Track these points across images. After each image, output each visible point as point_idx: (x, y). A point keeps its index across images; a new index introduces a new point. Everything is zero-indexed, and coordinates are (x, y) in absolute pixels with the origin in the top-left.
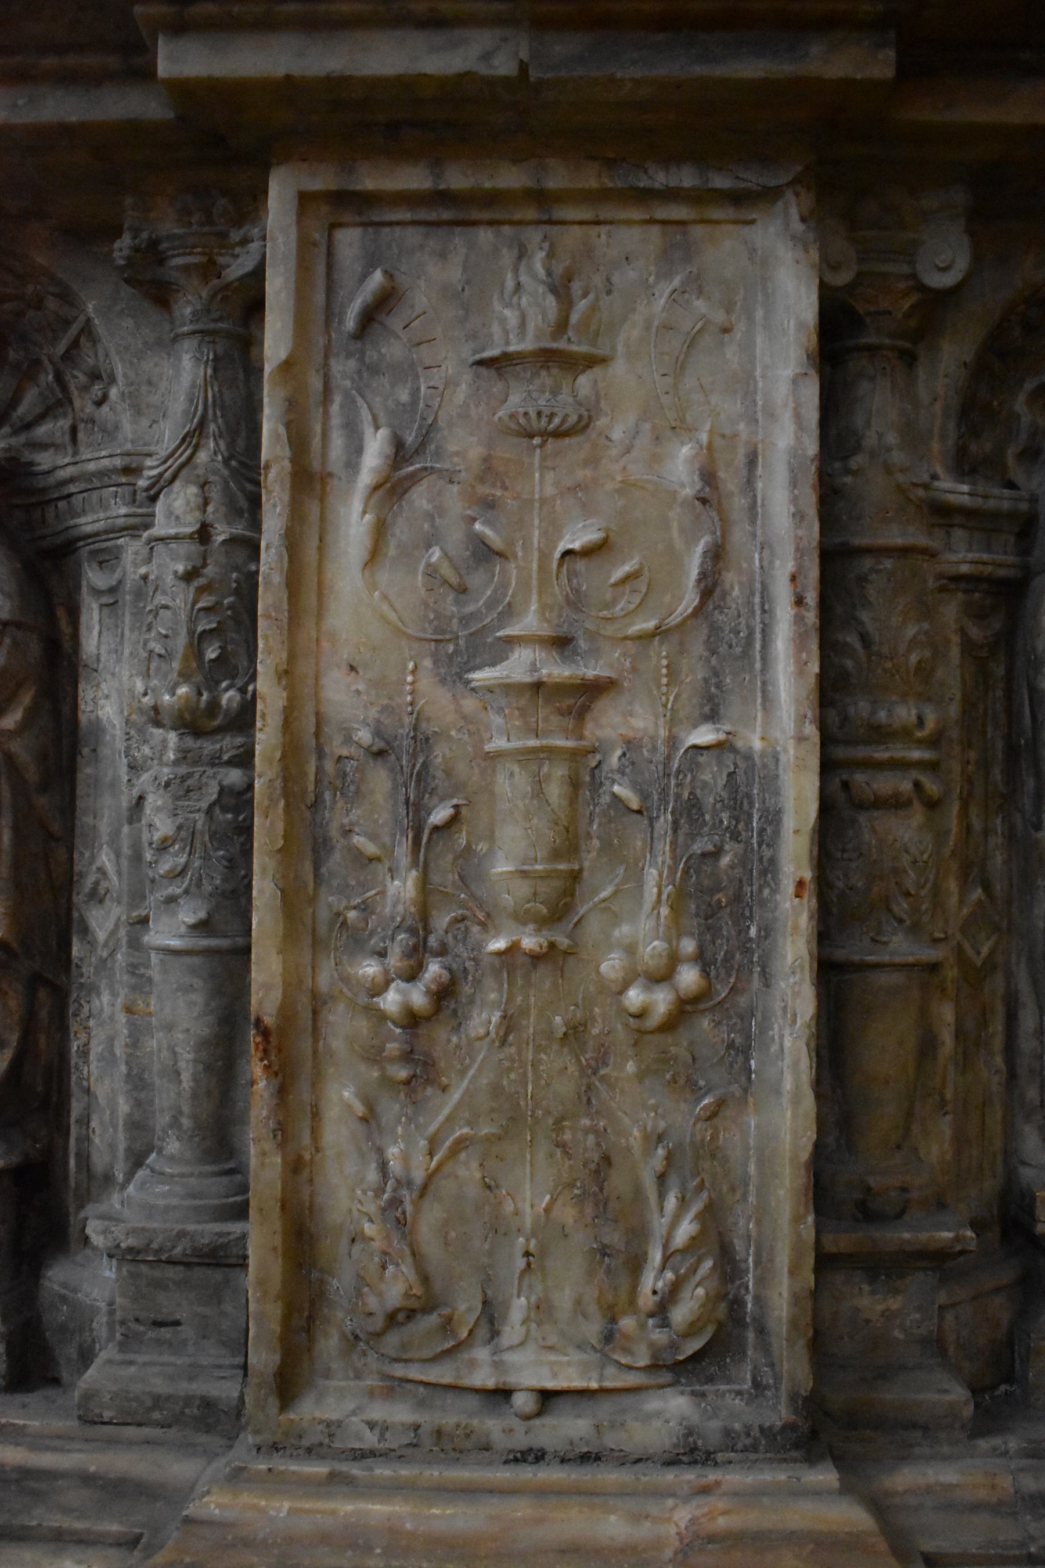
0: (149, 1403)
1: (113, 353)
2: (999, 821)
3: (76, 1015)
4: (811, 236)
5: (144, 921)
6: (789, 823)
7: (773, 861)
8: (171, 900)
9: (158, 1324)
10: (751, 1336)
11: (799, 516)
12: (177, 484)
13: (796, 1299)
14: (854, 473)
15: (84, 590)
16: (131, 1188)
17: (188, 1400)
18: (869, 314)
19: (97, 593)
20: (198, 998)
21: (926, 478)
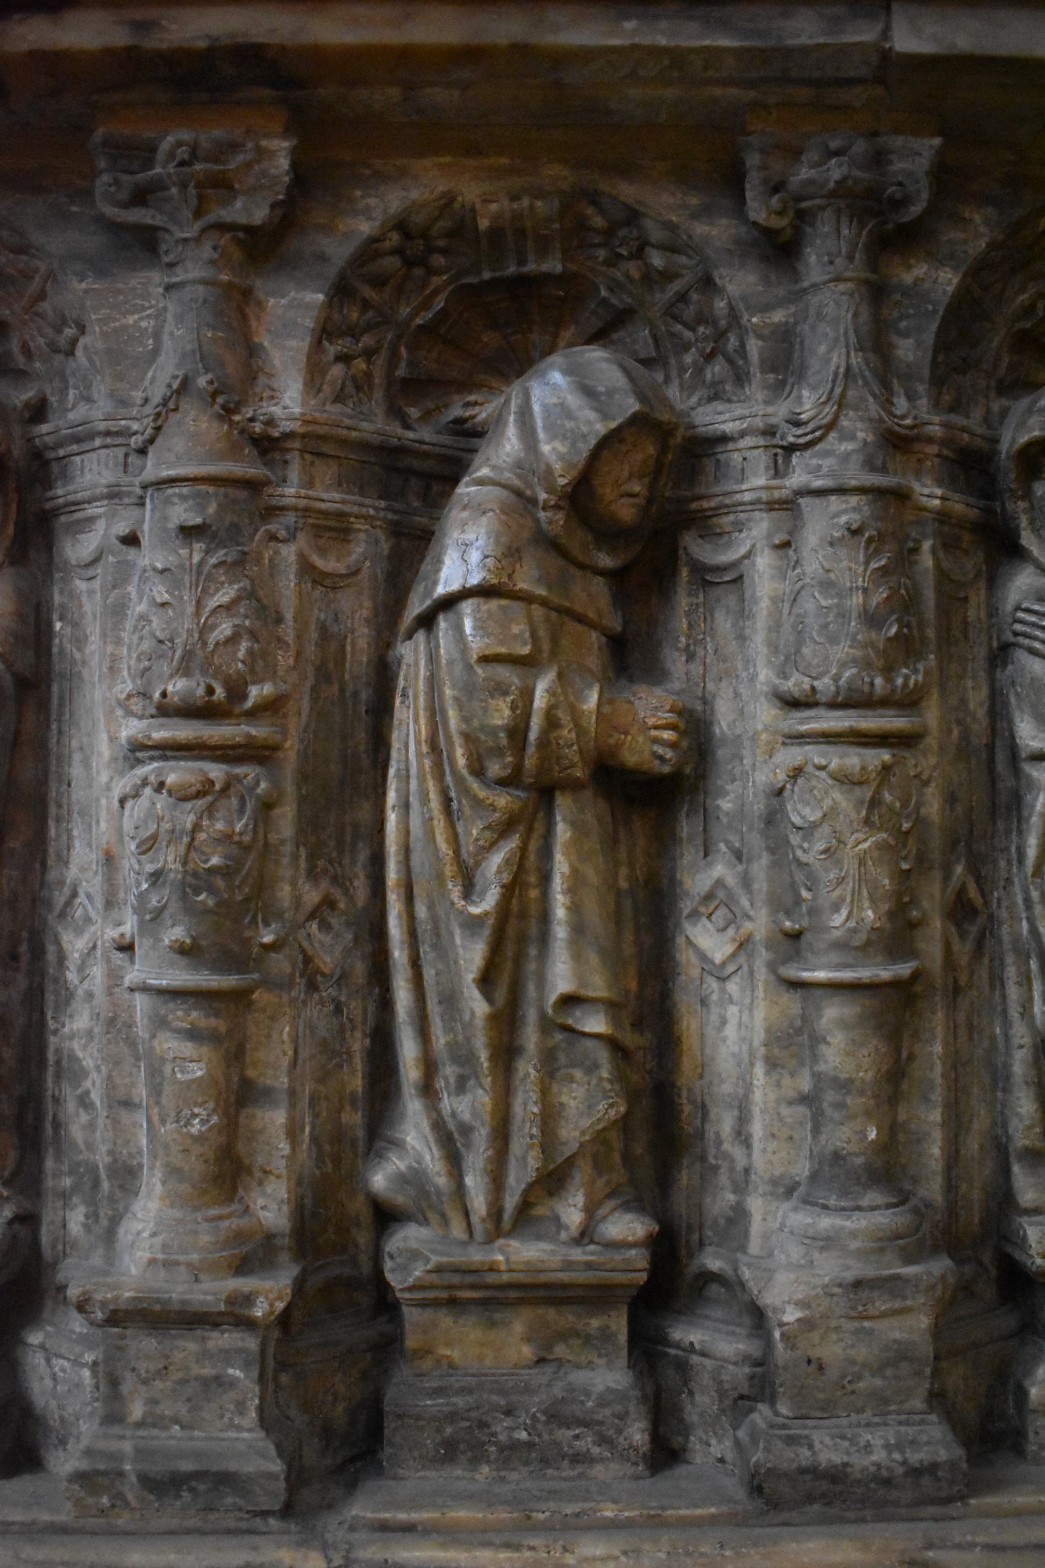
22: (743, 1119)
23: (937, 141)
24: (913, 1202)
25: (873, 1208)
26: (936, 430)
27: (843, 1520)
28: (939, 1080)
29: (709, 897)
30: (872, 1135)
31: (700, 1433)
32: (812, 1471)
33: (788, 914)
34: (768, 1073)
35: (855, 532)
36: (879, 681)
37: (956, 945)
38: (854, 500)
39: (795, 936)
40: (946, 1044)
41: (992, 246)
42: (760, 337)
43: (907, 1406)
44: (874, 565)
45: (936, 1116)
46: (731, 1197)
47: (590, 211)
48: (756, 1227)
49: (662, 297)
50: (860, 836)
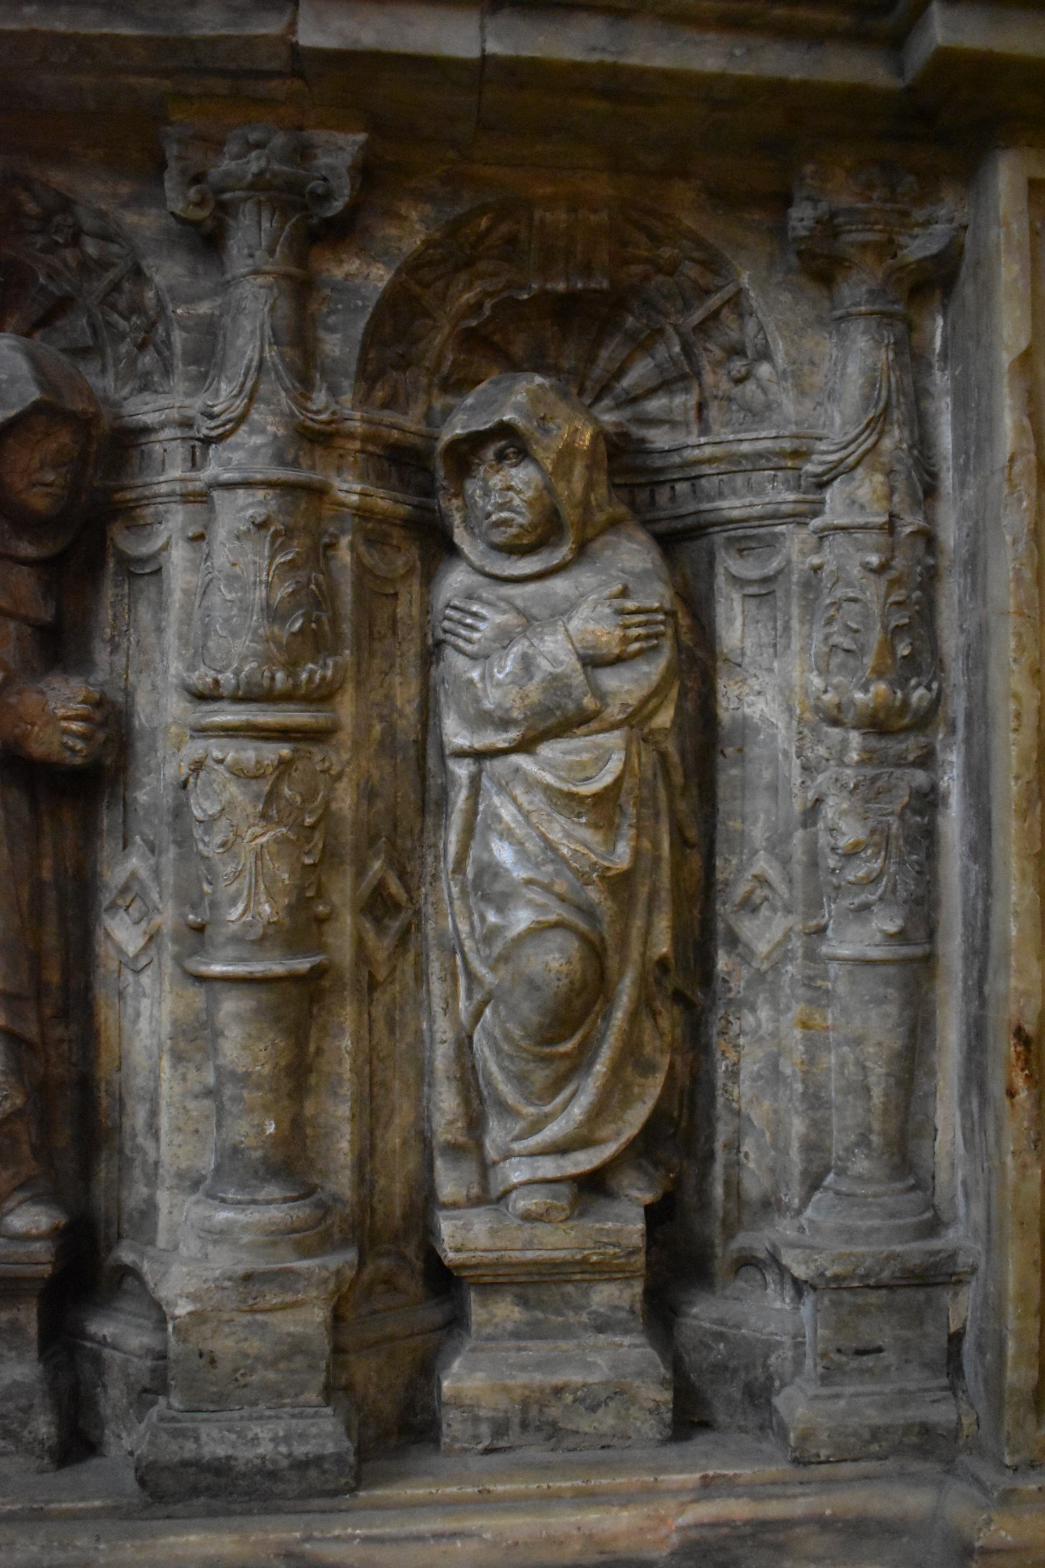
0: (867, 1435)
1: (771, 328)
3: (723, 1033)
5: (821, 930)
8: (866, 907)
9: (860, 1352)
12: (860, 472)
15: (721, 580)
16: (809, 1212)
17: (908, 1428)
19: (737, 581)
20: (892, 1009)
22: (154, 1113)
23: (361, 137)
24: (319, 1195)
25: (269, 1202)
26: (356, 426)
27: (229, 1513)
28: (347, 1075)
29: (125, 889)
30: (271, 1129)
31: (112, 1426)
32: (196, 1464)
33: (194, 907)
34: (174, 1067)
35: (262, 526)
36: (280, 676)
37: (371, 938)
38: (260, 494)
39: (200, 929)
40: (357, 1039)
41: (428, 244)
42: (184, 328)
43: (302, 1399)
44: (280, 559)
45: (344, 1110)
46: (144, 1191)
47: (23, 197)
48: (163, 1220)
49: (100, 286)
50: (258, 830)
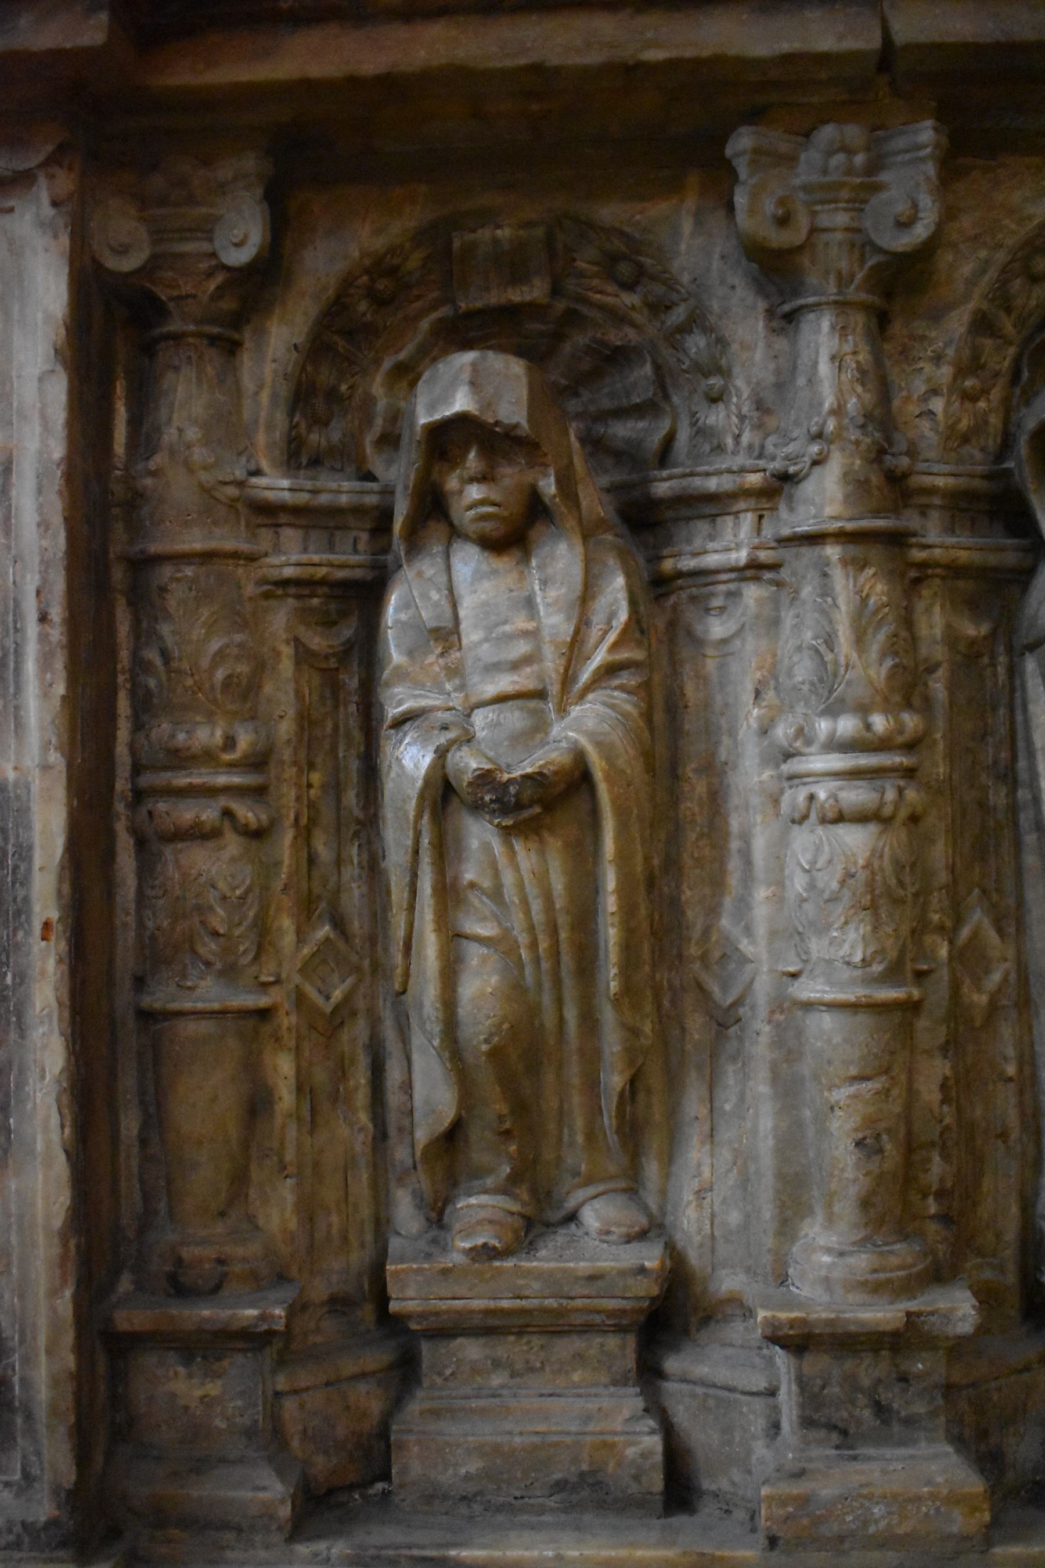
2: (355, 851)
4: (61, 222)
6: (38, 861)
7: (26, 900)
10: (19, 1421)
11: (44, 525)
13: (55, 1382)
14: (154, 474)
18: (172, 299)
21: (239, 474)
